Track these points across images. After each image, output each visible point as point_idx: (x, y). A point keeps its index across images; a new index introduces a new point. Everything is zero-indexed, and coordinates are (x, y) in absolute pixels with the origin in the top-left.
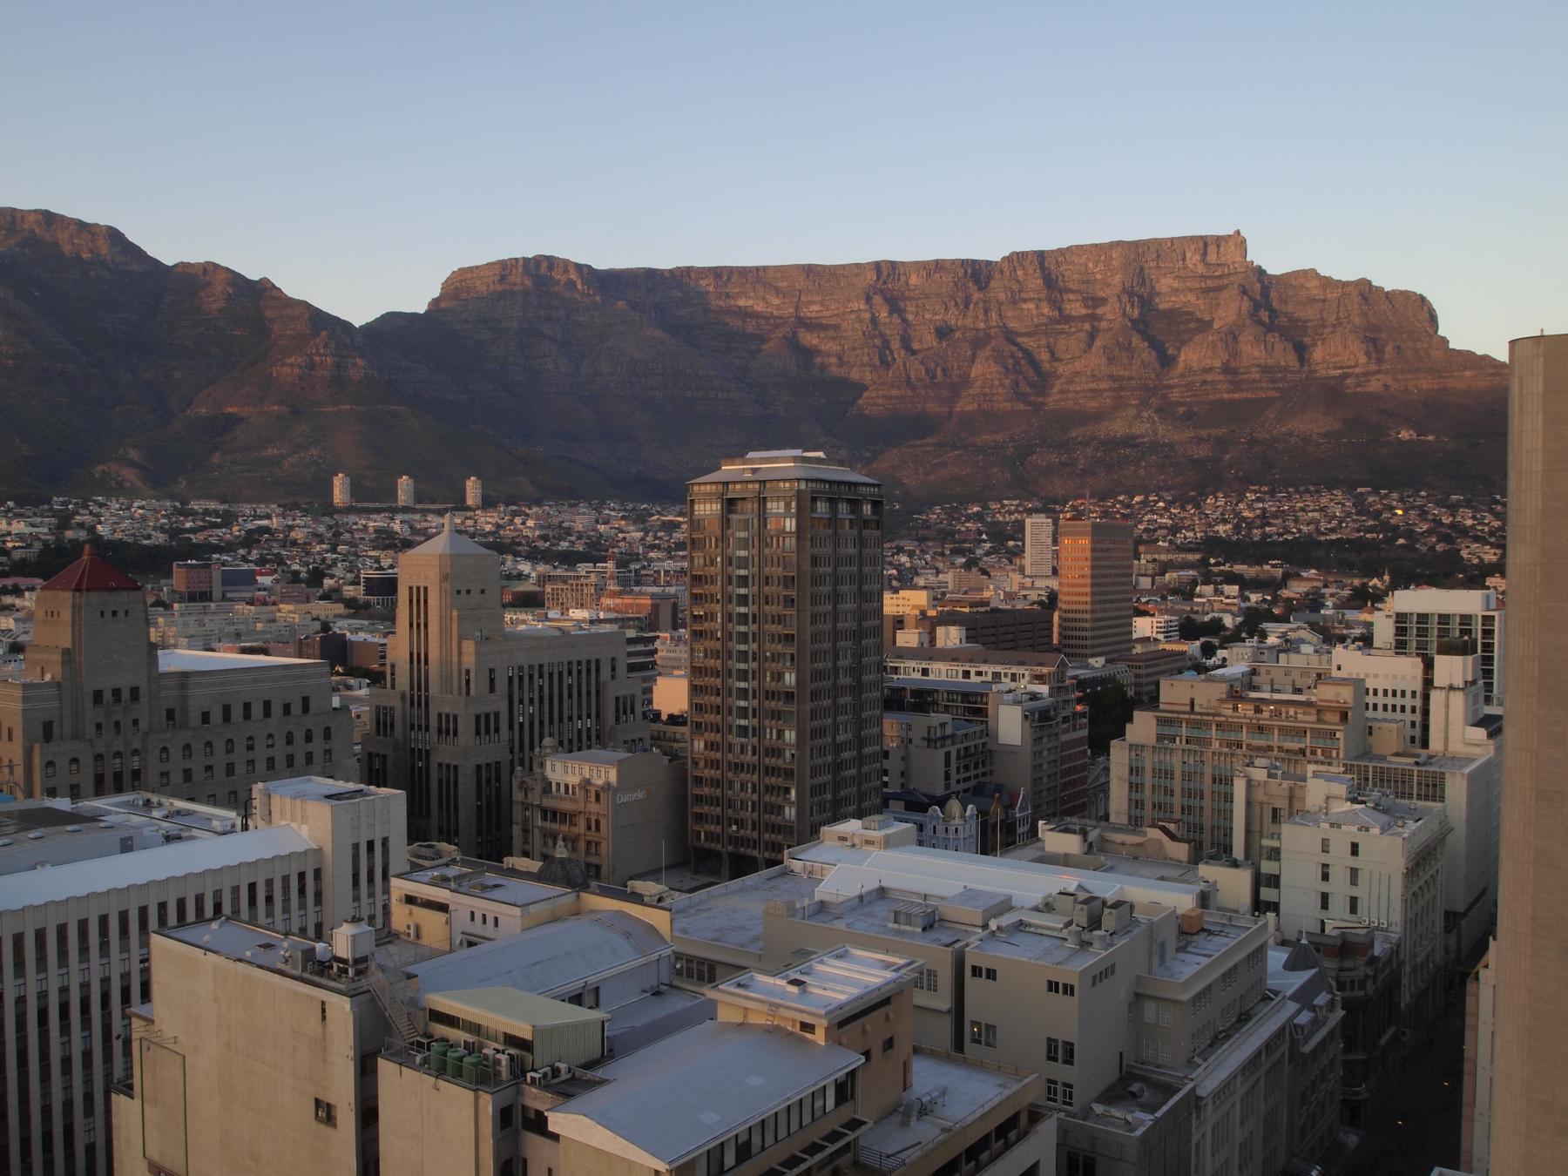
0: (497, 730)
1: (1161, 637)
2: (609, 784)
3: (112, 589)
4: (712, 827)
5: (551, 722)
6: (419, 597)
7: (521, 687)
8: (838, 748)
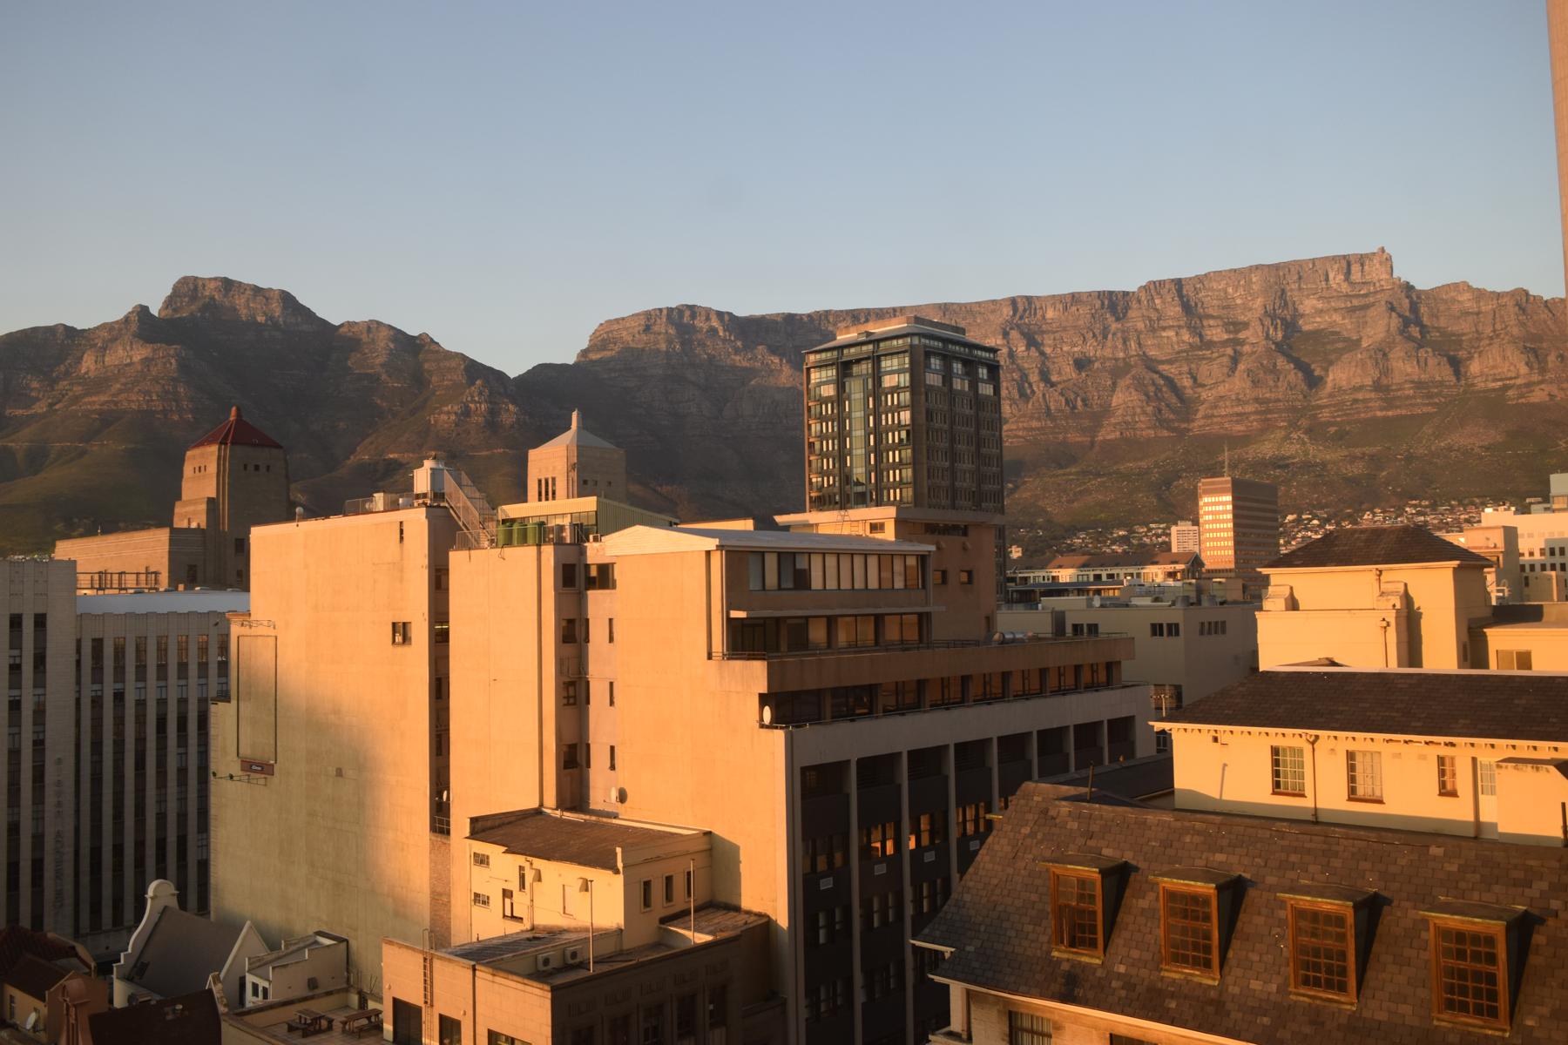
3: (254, 445)
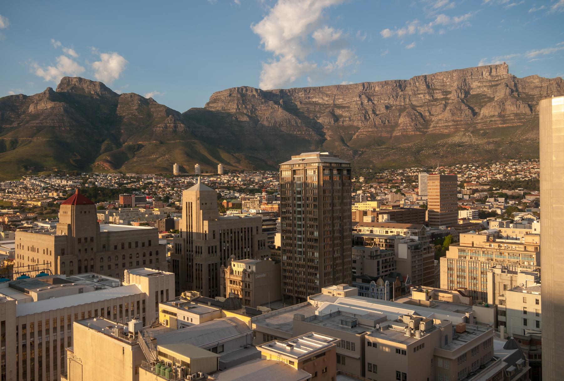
0: (216, 252)
1: (471, 218)
2: (252, 271)
3: (84, 204)
4: (290, 287)
5: (235, 249)
6: (189, 206)
7: (224, 237)
8: (335, 259)
